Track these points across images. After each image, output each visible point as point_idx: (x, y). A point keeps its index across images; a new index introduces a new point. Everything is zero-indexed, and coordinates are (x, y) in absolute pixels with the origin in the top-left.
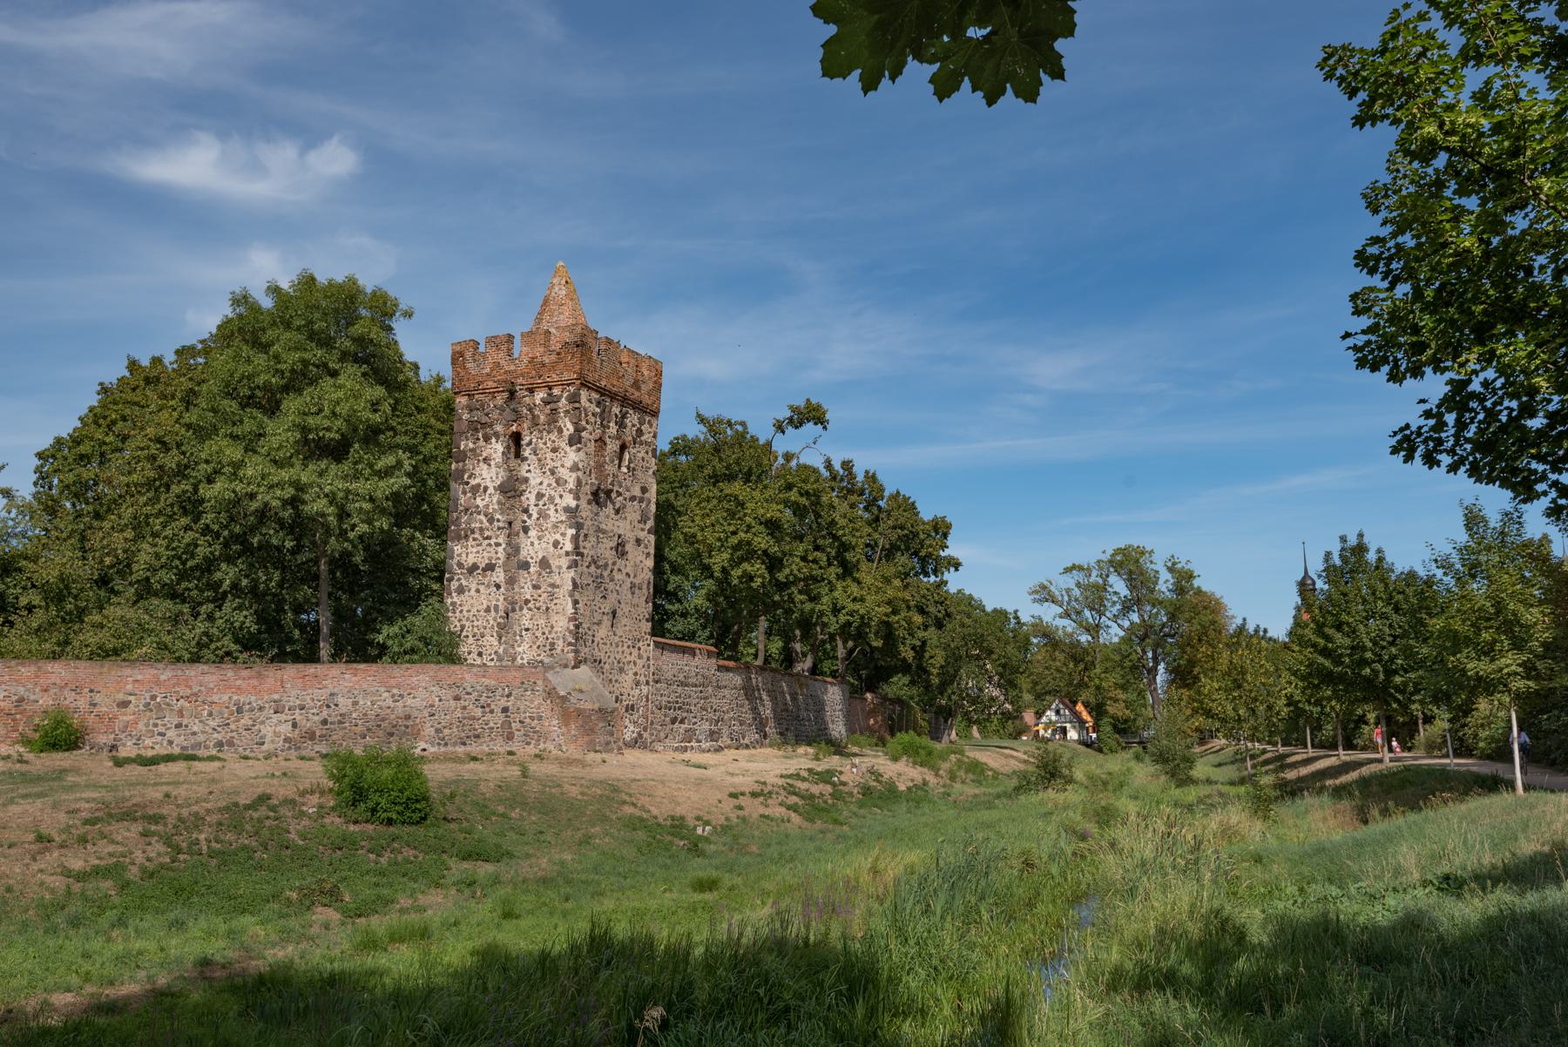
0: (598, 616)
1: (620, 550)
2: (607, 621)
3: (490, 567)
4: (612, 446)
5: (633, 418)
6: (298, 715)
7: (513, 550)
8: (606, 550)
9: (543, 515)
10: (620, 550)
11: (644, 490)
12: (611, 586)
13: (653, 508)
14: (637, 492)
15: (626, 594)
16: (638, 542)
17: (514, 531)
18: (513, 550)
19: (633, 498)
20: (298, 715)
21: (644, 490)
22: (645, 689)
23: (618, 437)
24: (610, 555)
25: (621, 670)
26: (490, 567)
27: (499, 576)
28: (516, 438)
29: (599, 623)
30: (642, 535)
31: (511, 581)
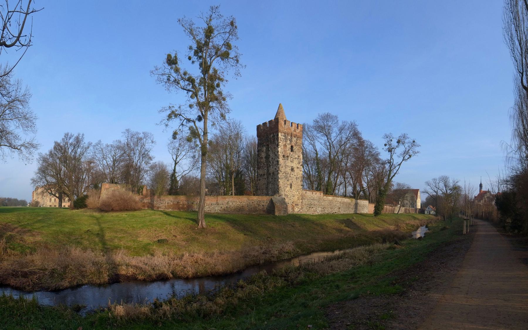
0: (286, 185)
1: (292, 169)
2: (289, 186)
3: (264, 175)
4: (289, 146)
5: (294, 139)
6: (222, 206)
7: (268, 170)
8: (288, 170)
9: (273, 163)
10: (292, 169)
11: (299, 156)
12: (290, 178)
13: (302, 160)
14: (297, 156)
15: (294, 179)
16: (298, 168)
17: (268, 166)
18: (268, 170)
19: (296, 158)
20: (222, 206)
21: (299, 156)
22: (301, 201)
23: (290, 144)
24: (289, 171)
25: (294, 196)
26: (264, 175)
27: (266, 177)
28: (268, 145)
29: (287, 187)
30: (299, 166)
31: (268, 177)
